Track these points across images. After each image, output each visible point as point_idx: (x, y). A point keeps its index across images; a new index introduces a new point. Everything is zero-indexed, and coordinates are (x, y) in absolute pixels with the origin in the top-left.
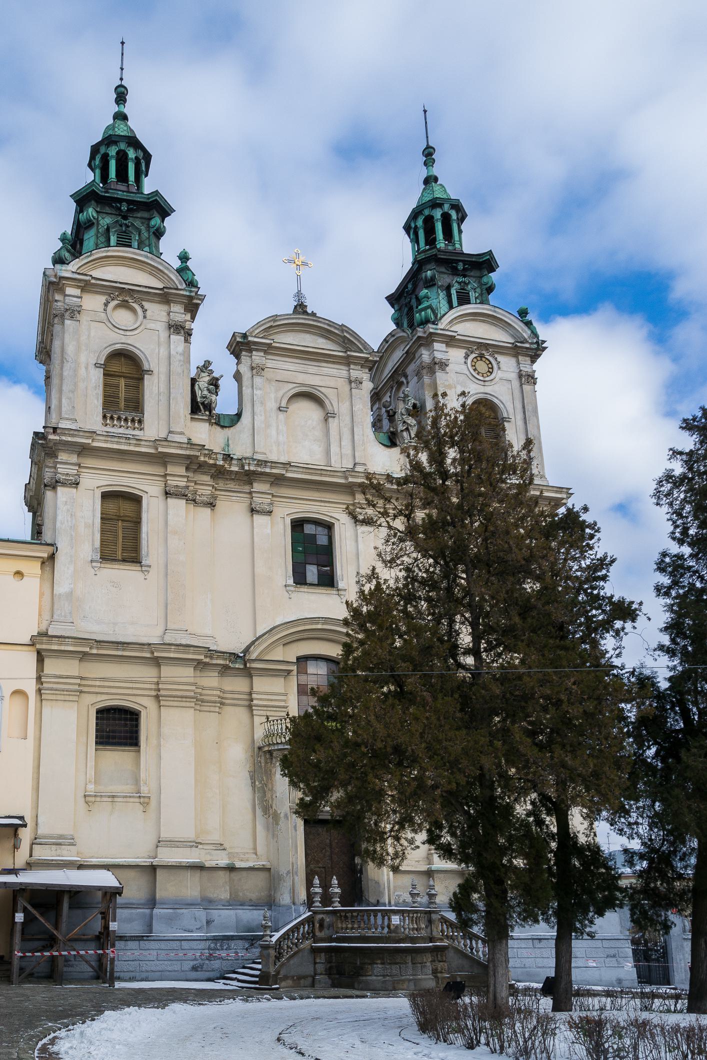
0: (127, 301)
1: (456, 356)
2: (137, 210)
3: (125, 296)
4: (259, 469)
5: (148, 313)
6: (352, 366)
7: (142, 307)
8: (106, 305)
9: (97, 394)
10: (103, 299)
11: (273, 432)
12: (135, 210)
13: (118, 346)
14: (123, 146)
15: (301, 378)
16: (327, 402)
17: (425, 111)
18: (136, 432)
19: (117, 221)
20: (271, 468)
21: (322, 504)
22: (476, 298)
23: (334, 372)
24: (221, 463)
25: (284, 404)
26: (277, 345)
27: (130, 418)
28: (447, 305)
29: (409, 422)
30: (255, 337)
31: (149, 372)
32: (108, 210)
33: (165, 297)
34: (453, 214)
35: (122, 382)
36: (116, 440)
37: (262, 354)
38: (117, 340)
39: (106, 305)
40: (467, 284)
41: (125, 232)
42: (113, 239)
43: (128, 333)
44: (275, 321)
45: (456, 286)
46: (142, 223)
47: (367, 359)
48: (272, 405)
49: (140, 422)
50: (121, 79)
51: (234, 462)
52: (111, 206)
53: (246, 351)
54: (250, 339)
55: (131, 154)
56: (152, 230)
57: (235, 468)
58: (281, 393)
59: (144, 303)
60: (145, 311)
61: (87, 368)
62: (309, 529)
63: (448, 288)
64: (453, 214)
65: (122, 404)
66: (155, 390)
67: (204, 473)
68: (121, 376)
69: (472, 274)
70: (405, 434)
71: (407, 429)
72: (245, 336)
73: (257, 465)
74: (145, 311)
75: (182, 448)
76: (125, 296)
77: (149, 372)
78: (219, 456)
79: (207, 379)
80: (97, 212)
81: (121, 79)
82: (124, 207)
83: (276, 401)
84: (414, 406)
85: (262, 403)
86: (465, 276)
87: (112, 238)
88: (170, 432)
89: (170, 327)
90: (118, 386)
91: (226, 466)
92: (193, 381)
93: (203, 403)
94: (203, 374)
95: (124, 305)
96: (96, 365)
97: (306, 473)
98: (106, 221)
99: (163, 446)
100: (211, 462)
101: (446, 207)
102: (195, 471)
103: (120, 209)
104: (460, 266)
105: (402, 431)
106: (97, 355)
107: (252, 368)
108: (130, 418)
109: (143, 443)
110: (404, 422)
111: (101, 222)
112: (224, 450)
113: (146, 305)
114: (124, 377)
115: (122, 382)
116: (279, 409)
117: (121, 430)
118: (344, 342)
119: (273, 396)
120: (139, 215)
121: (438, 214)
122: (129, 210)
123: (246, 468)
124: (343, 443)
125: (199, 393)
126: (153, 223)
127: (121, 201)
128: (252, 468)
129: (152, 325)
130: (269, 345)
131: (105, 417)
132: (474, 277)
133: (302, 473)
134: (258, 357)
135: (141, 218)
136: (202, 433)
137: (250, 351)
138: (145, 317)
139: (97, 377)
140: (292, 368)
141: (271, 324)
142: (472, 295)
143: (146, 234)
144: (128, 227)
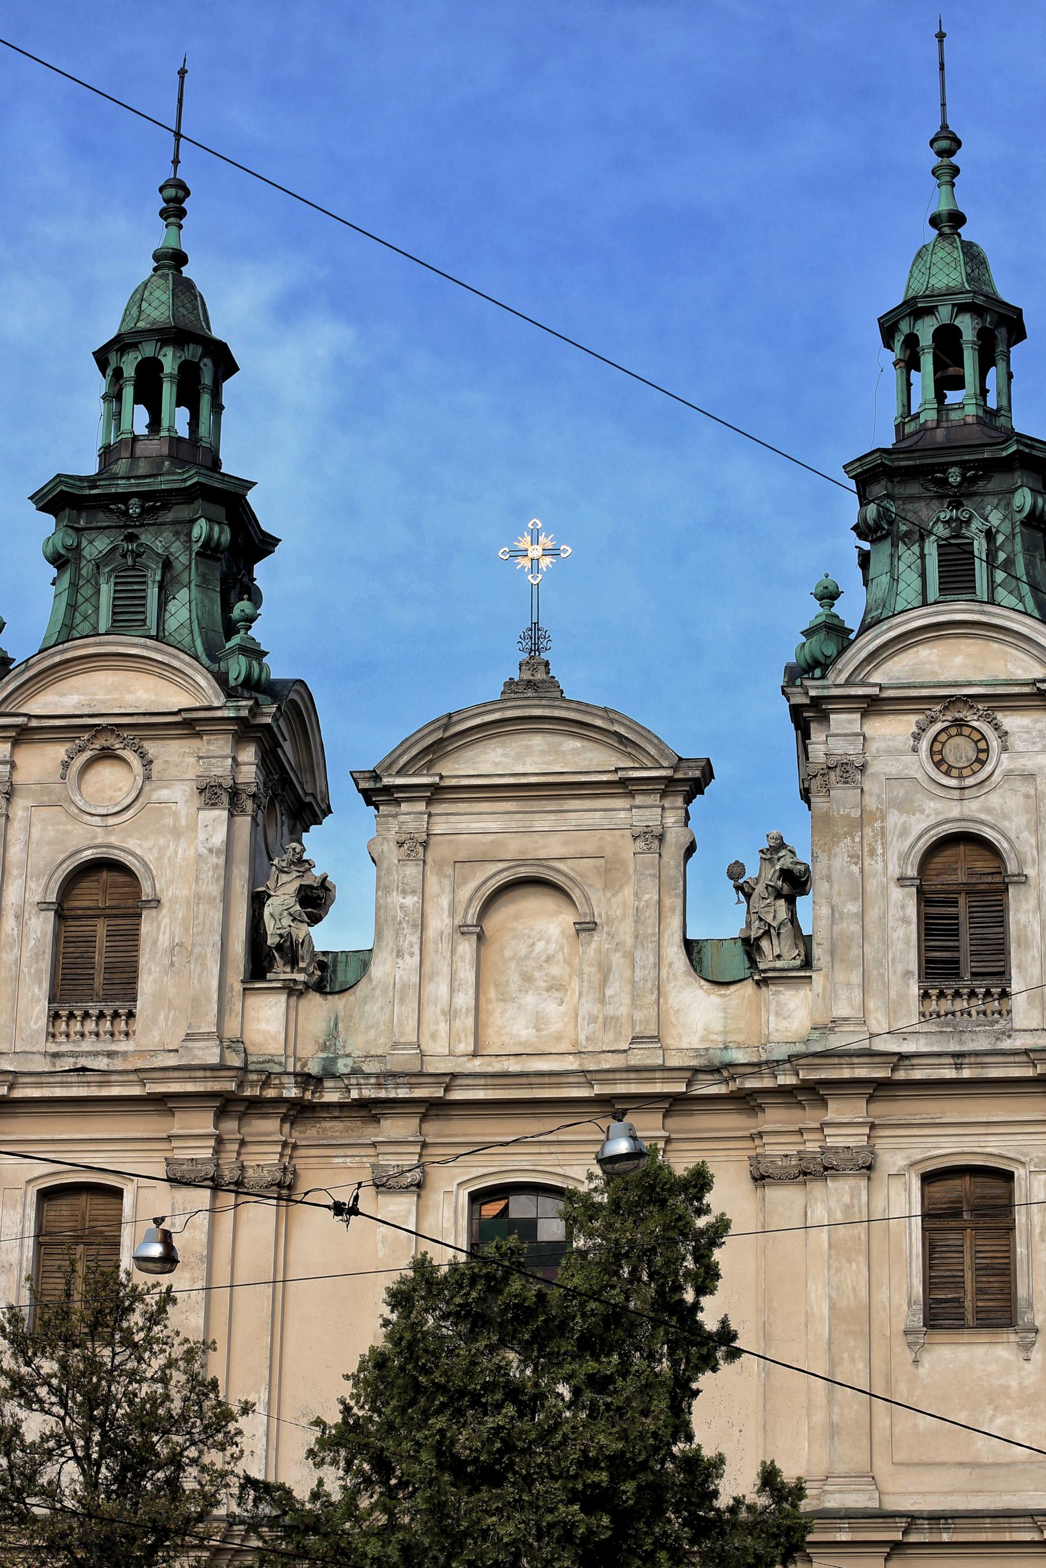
0: (109, 748)
1: (893, 731)
2: (166, 507)
3: (103, 738)
4: (382, 1094)
5: (156, 767)
6: (639, 800)
7: (142, 756)
8: (66, 765)
9: (39, 971)
10: (59, 752)
11: (444, 990)
12: (160, 508)
13: (88, 855)
14: (148, 350)
15: (514, 847)
16: (576, 894)
17: (941, 36)
18: (122, 1046)
19: (114, 549)
20: (412, 1086)
21: (544, 1149)
22: (991, 555)
23: (596, 818)
24: (292, 1092)
25: (471, 919)
26: (453, 782)
27: (108, 1012)
28: (917, 584)
29: (769, 919)
30: (399, 773)
31: (156, 903)
32: (102, 519)
33: (189, 725)
34: (967, 326)
35: (101, 928)
36: (58, 1079)
37: (421, 806)
38: (85, 840)
39: (66, 765)
40: (968, 522)
41: (133, 568)
42: (106, 591)
43: (111, 821)
44: (446, 727)
45: (941, 530)
46: (177, 534)
47: (670, 781)
48: (439, 922)
49: (131, 1015)
50: (176, 162)
51: (328, 1084)
52: (107, 509)
53: (387, 803)
54: (387, 781)
55: (169, 361)
56: (196, 547)
57: (331, 1097)
58: (465, 893)
59: (147, 745)
60: (148, 763)
61: (19, 917)
62: (521, 1207)
63: (922, 539)
64: (967, 326)
65: (99, 979)
66: (164, 940)
67: (265, 1116)
68: (98, 917)
69: (991, 486)
70: (765, 944)
71: (767, 933)
72: (375, 776)
73: (379, 1086)
74: (148, 763)
75: (194, 1079)
76: (103, 738)
77: (156, 903)
78: (285, 1079)
79: (296, 884)
80: (77, 530)
81: (176, 162)
82: (134, 510)
83: (452, 913)
84: (786, 874)
85: (415, 926)
86: (957, 505)
87: (104, 588)
88: (189, 1037)
89: (202, 791)
90: (90, 941)
91: (308, 1096)
92: (258, 900)
93: (279, 947)
94: (284, 878)
95: (107, 755)
96: (43, 906)
97: (495, 1087)
98: (97, 546)
99: (154, 1081)
100: (271, 1093)
101: (944, 314)
102: (242, 1117)
103: (126, 513)
104: (954, 476)
105: (758, 939)
106: (43, 881)
107: (400, 844)
108: (108, 1012)
109: (113, 1078)
110: (761, 919)
111: (85, 553)
112: (324, 1048)
113: (152, 748)
114: (106, 916)
115: (101, 928)
116: (462, 930)
117: (86, 1046)
118: (621, 742)
119: (445, 901)
120: (170, 516)
121: (926, 331)
122: (145, 511)
123: (354, 1094)
124: (609, 992)
125: (270, 925)
126: (196, 532)
127: (124, 498)
128: (368, 1093)
129: (164, 794)
130: (435, 788)
131: (55, 1016)
132: (994, 494)
133: (485, 1087)
134: (410, 815)
135: (174, 523)
136: (267, 1021)
137: (398, 802)
138: (148, 778)
139: (42, 927)
140: (493, 825)
141: (439, 735)
142: (980, 546)
143: (184, 559)
144: (140, 555)
